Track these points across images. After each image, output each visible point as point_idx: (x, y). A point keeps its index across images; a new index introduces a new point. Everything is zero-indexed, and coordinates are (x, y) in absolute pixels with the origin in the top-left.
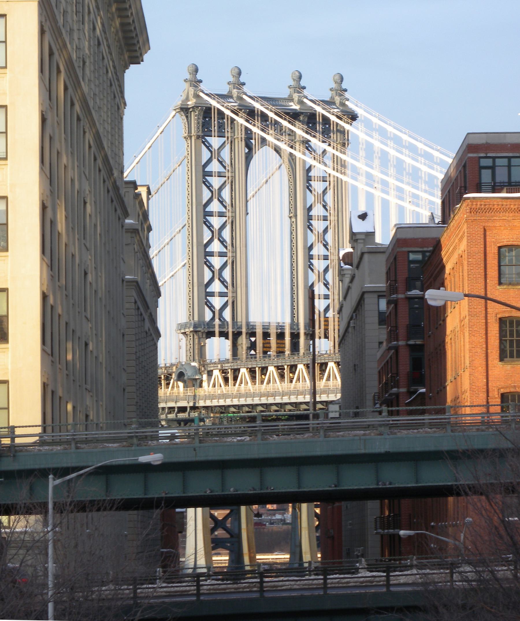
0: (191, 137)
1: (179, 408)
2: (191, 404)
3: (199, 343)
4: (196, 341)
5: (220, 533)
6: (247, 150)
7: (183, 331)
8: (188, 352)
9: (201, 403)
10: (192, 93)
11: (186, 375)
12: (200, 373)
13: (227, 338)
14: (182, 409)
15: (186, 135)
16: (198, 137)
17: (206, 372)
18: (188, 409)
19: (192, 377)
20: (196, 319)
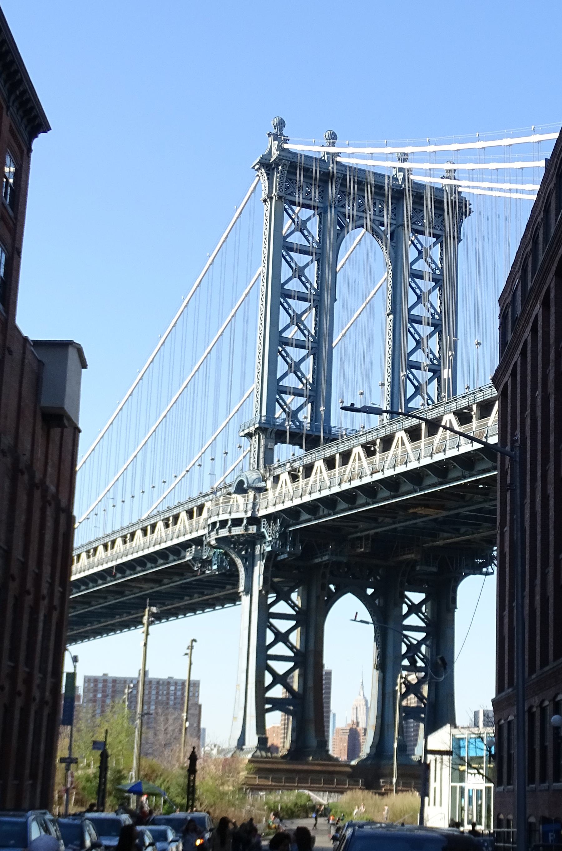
0: (271, 198)
1: (233, 520)
2: (249, 514)
3: (266, 446)
4: (262, 442)
5: (278, 692)
6: (338, 228)
7: (246, 431)
8: (252, 460)
9: (262, 513)
10: (276, 146)
11: (245, 481)
12: (265, 481)
13: (301, 447)
14: (237, 522)
15: (264, 196)
16: (280, 198)
17: (272, 478)
18: (245, 522)
19: (254, 485)
20: (264, 412)
